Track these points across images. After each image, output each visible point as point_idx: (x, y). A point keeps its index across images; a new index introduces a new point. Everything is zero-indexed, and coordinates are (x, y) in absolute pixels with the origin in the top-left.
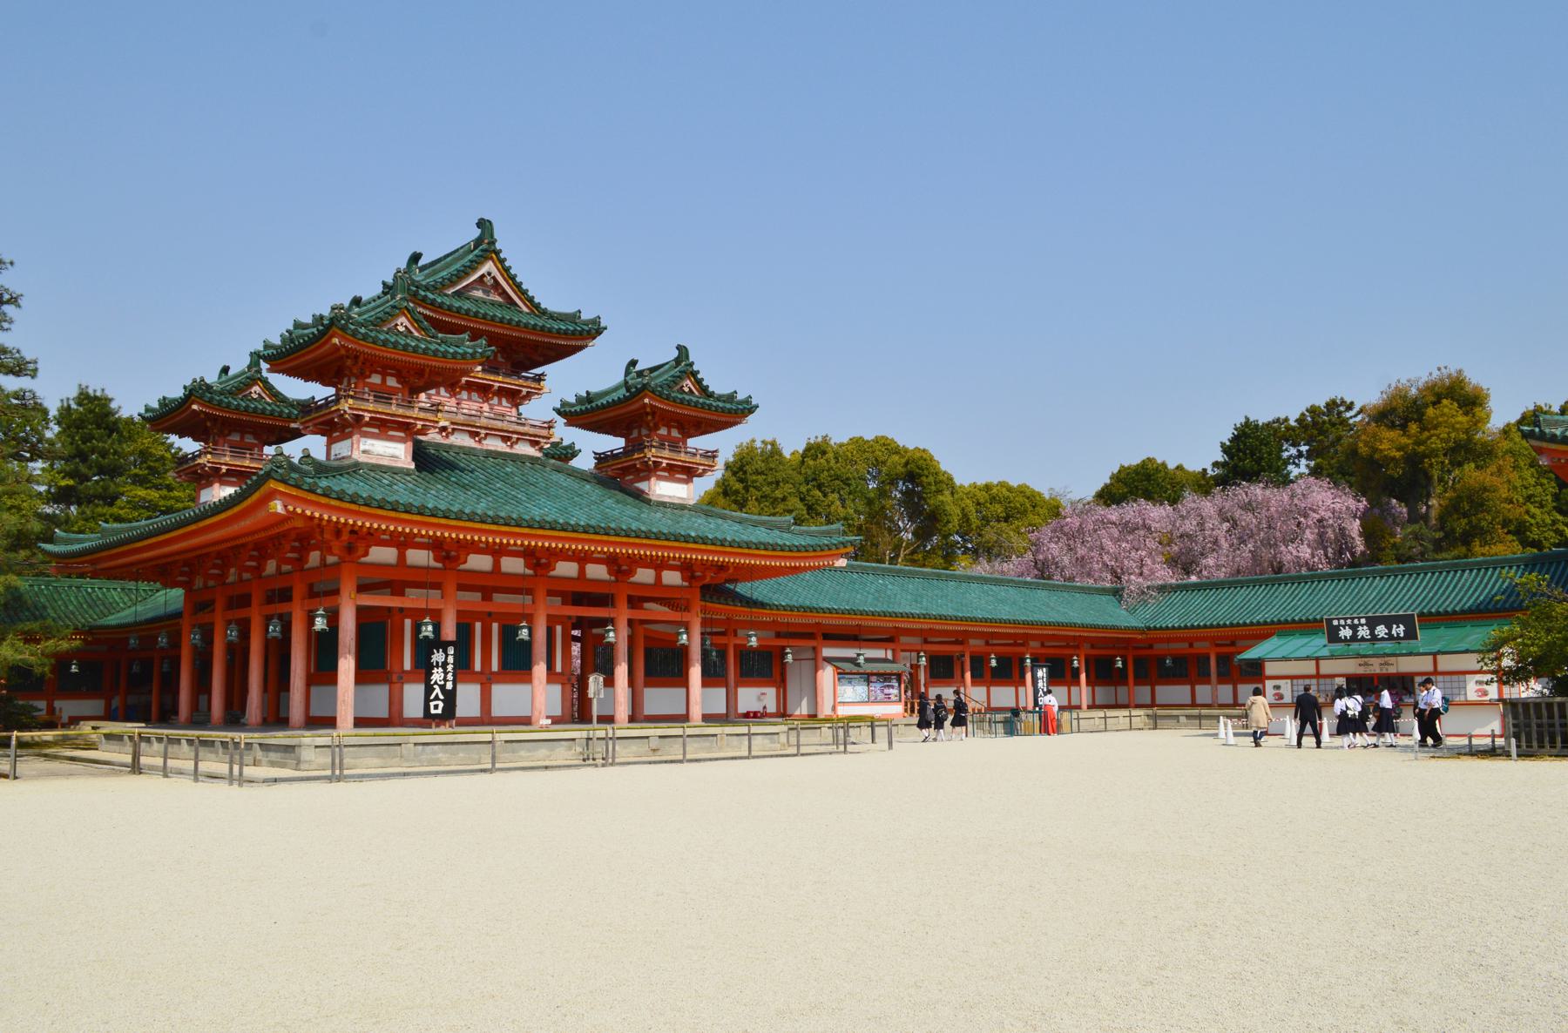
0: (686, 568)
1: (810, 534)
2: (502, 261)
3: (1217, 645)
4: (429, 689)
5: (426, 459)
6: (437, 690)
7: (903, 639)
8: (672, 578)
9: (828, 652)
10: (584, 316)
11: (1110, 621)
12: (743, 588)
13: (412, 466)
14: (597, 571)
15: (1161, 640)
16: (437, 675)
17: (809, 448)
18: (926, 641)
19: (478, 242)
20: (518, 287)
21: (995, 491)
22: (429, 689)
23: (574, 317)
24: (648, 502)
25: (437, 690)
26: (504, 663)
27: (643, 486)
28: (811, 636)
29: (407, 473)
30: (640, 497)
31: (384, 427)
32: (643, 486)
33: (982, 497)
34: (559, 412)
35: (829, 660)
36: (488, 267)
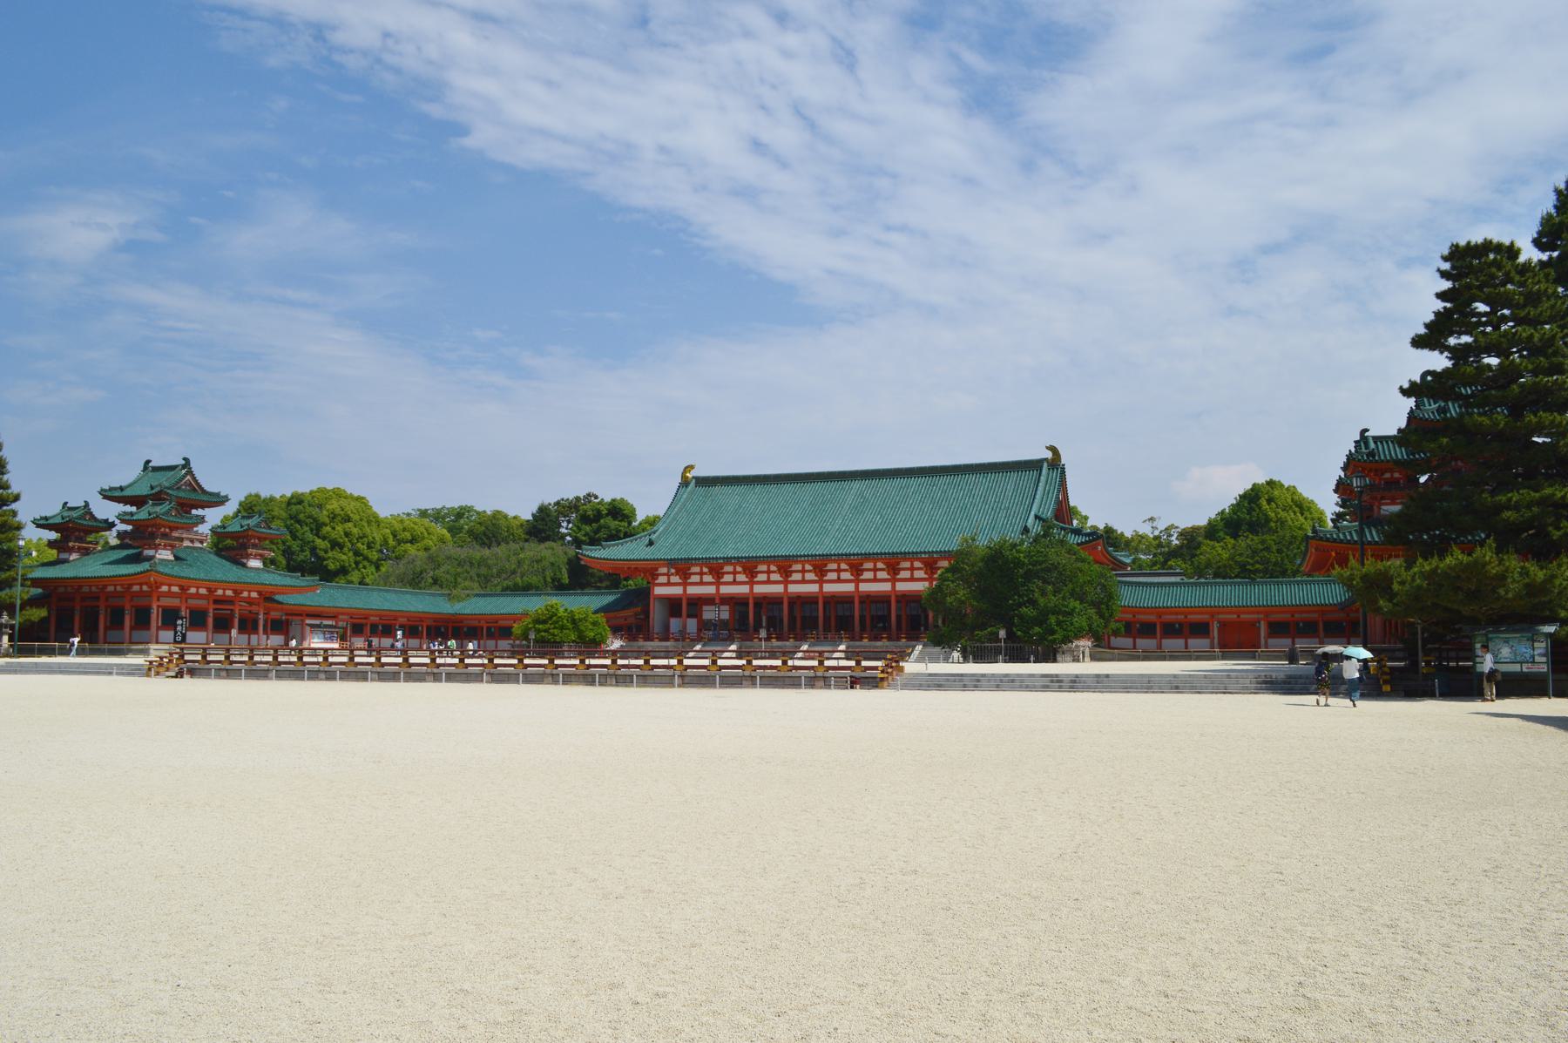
0: (260, 593)
1: (307, 581)
2: (193, 475)
3: (487, 623)
4: (176, 633)
5: (177, 558)
6: (179, 633)
7: (341, 617)
8: (254, 595)
9: (308, 621)
10: (222, 494)
11: (437, 610)
12: (277, 597)
13: (173, 558)
14: (229, 593)
15: (467, 619)
16: (179, 628)
17: (292, 497)
18: (351, 618)
19: (184, 467)
20: (198, 484)
21: (405, 524)
22: (176, 633)
23: (218, 495)
24: (247, 567)
25: (179, 633)
26: (163, 623)
27: (245, 561)
28: (301, 615)
29: (172, 561)
30: (244, 565)
31: (165, 547)
32: (245, 561)
33: (398, 526)
34: (211, 530)
35: (307, 624)
36: (188, 477)
